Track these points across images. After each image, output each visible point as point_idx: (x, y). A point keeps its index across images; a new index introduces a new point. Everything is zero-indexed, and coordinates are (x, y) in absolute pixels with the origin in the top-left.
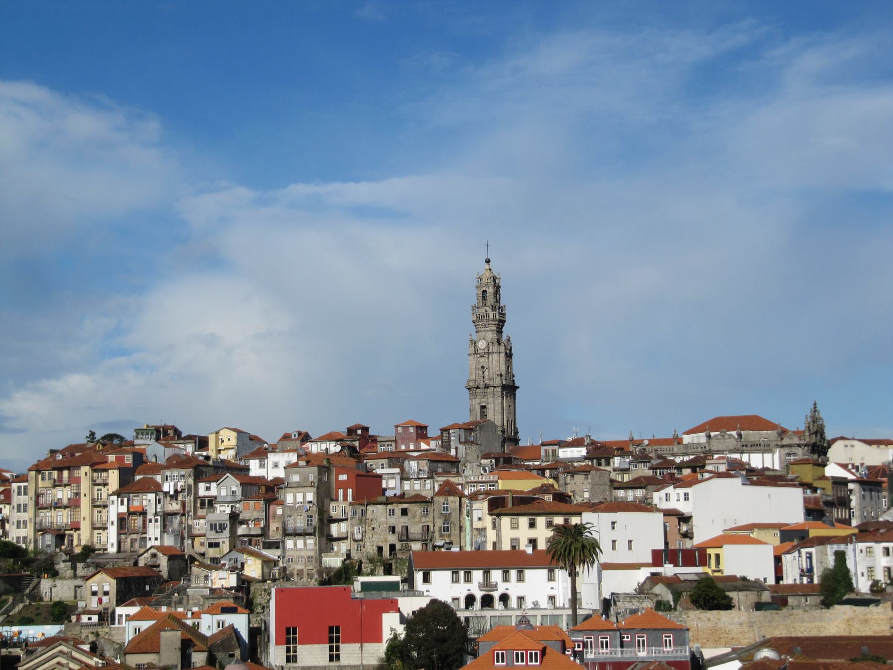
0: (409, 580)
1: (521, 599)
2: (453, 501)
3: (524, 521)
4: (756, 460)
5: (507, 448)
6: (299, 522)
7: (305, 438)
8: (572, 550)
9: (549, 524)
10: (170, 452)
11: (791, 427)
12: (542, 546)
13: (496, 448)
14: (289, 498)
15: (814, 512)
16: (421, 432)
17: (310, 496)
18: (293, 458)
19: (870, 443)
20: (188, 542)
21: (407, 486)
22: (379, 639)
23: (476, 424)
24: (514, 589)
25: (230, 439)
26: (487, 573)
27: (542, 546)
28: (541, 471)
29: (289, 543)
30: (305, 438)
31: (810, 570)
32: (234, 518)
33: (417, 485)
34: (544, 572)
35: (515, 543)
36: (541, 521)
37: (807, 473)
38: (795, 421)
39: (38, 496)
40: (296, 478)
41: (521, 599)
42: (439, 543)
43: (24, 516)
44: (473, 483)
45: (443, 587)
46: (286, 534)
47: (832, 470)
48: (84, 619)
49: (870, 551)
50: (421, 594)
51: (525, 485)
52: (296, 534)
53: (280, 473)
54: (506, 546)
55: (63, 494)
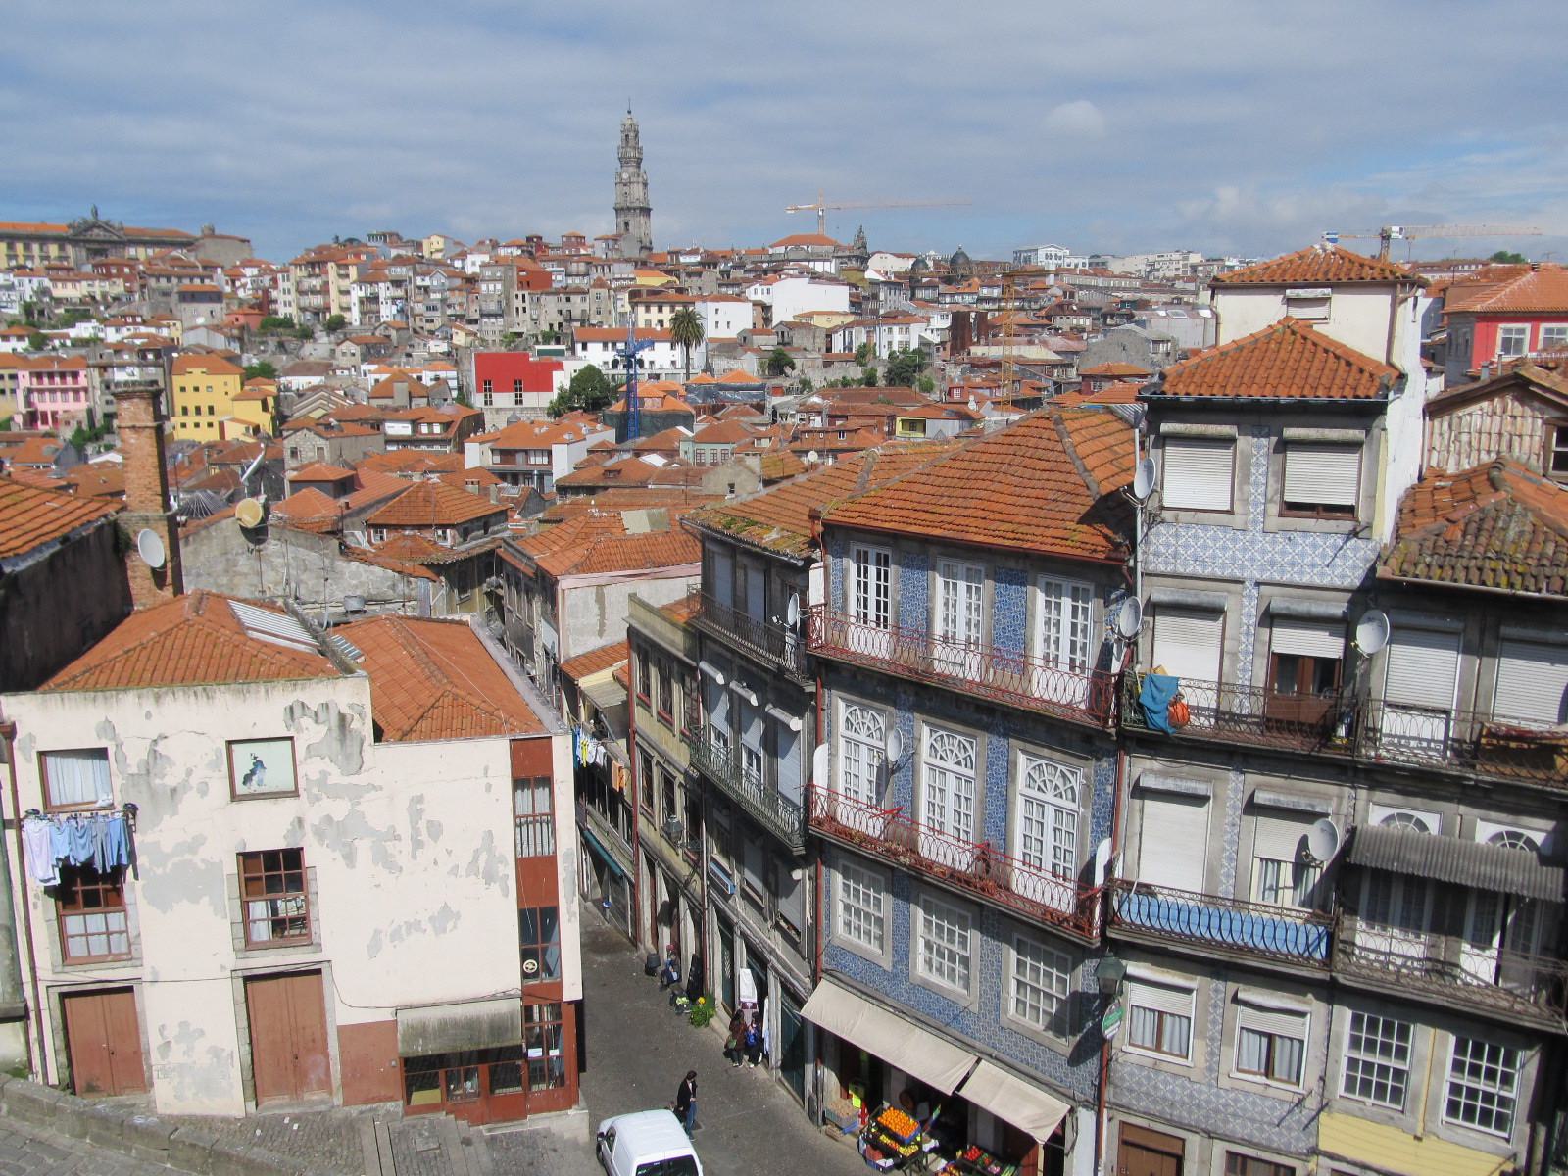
0: (573, 349)
2: (603, 292)
3: (654, 309)
4: (819, 267)
5: (644, 254)
6: (493, 307)
8: (686, 331)
9: (672, 310)
10: (394, 252)
11: (844, 243)
12: (667, 325)
13: (635, 254)
14: (484, 287)
15: (856, 303)
17: (499, 286)
18: (486, 258)
19: (898, 256)
20: (411, 319)
21: (570, 281)
22: (549, 388)
23: (621, 236)
27: (667, 325)
28: (669, 272)
29: (486, 320)
30: (495, 245)
31: (851, 342)
32: (443, 300)
33: (578, 280)
34: (669, 345)
35: (648, 322)
36: (666, 309)
37: (854, 277)
38: (847, 239)
39: (298, 284)
40: (488, 274)
41: (652, 362)
42: (594, 322)
43: (289, 298)
44: (617, 280)
45: (597, 356)
46: (483, 315)
47: (870, 275)
48: (338, 372)
49: (890, 331)
50: (580, 359)
51: (656, 281)
52: (489, 315)
53: (477, 270)
54: (641, 325)
55: (317, 283)
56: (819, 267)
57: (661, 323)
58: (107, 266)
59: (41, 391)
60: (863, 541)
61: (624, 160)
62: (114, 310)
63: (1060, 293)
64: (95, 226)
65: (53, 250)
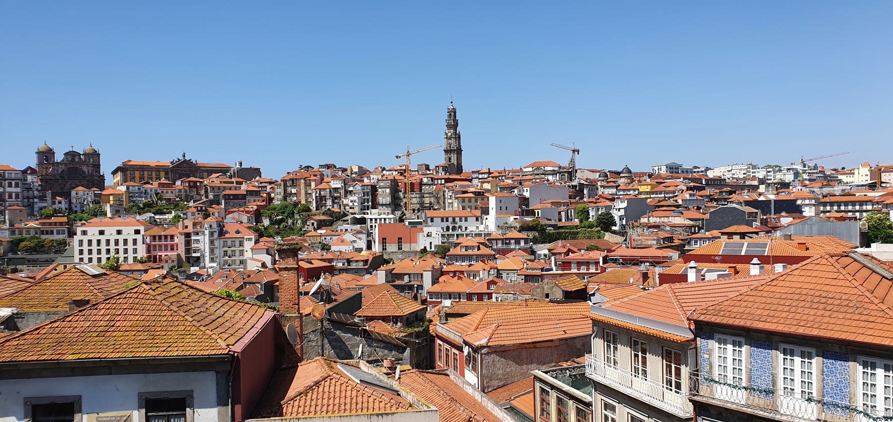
1: (466, 228)
7: (384, 169)
11: (563, 165)
16: (427, 168)
17: (388, 191)
19: (590, 171)
24: (464, 224)
25: (356, 169)
26: (454, 219)
30: (384, 169)
56: (550, 178)
57: (470, 207)
58: (190, 182)
59: (155, 246)
60: (723, 333)
61: (449, 126)
62: (191, 204)
63: (685, 188)
64: (185, 161)
65: (162, 174)
